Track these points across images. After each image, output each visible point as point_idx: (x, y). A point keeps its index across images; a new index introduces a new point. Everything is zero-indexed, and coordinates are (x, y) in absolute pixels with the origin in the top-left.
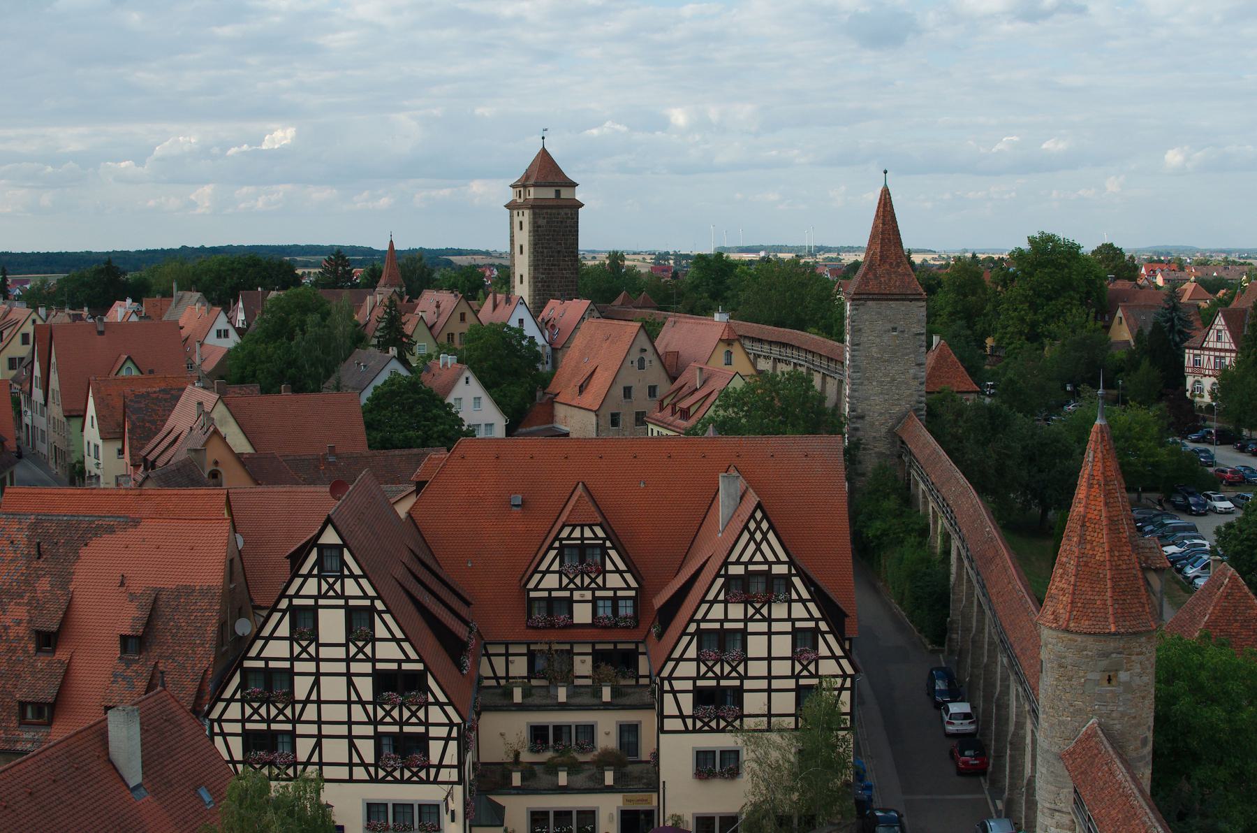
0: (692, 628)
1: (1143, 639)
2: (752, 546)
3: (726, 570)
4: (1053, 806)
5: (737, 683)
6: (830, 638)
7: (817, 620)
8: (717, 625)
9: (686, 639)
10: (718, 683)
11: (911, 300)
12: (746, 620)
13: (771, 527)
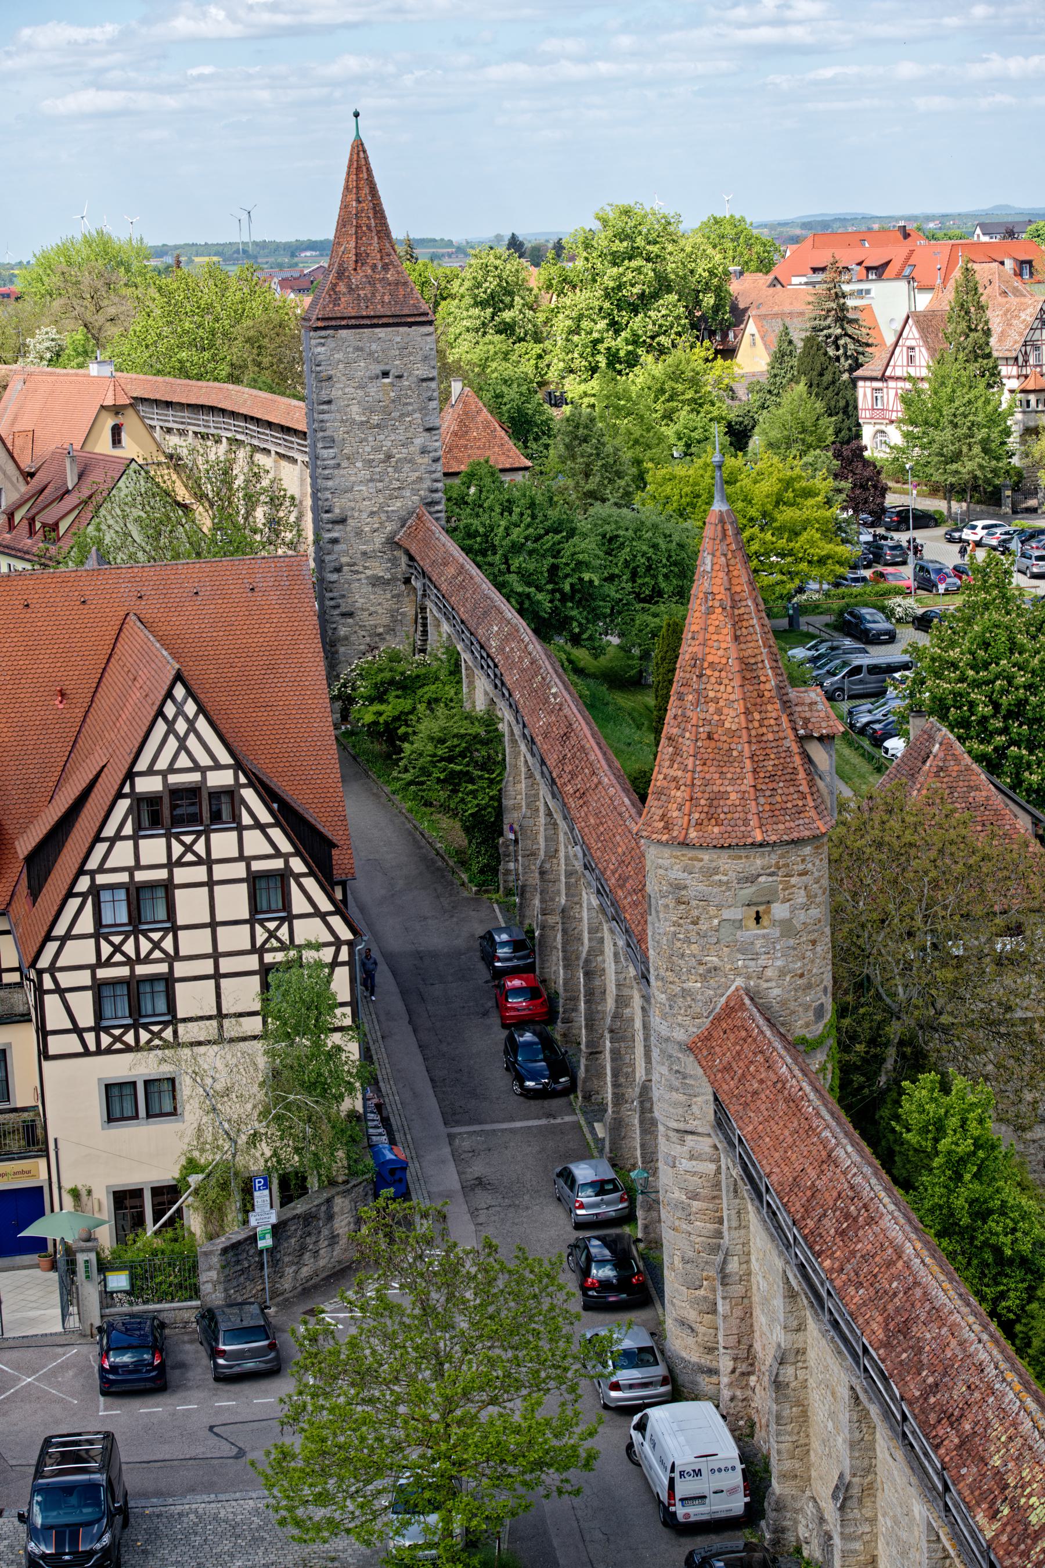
0: (83, 884)
1: (808, 850)
2: (172, 744)
3: (133, 786)
4: (682, 1126)
5: (163, 968)
6: (310, 883)
7: (286, 857)
8: (124, 877)
9: (74, 903)
10: (132, 970)
11: (410, 325)
12: (171, 865)
13: (201, 710)
